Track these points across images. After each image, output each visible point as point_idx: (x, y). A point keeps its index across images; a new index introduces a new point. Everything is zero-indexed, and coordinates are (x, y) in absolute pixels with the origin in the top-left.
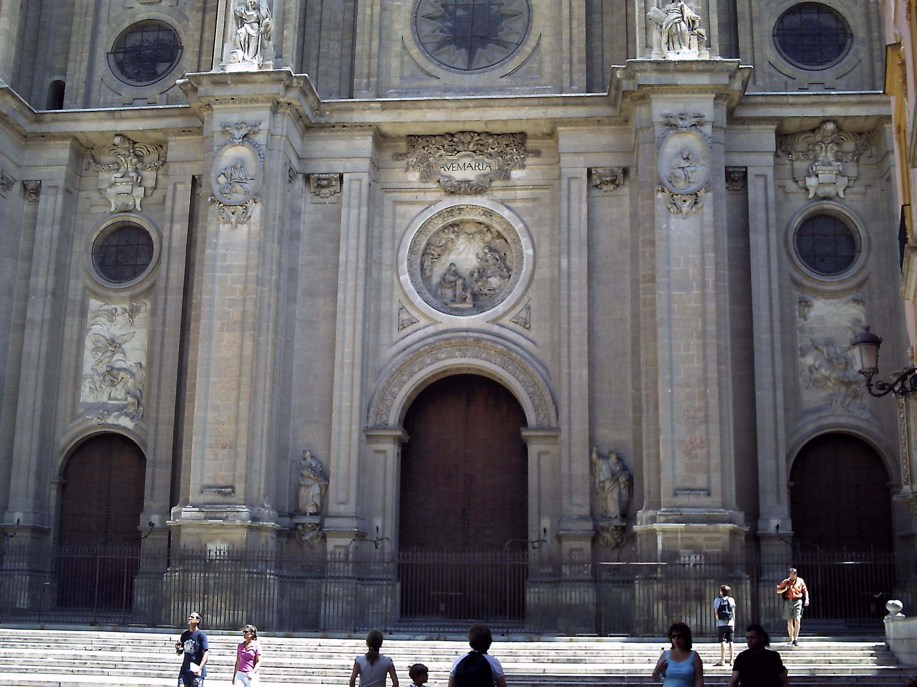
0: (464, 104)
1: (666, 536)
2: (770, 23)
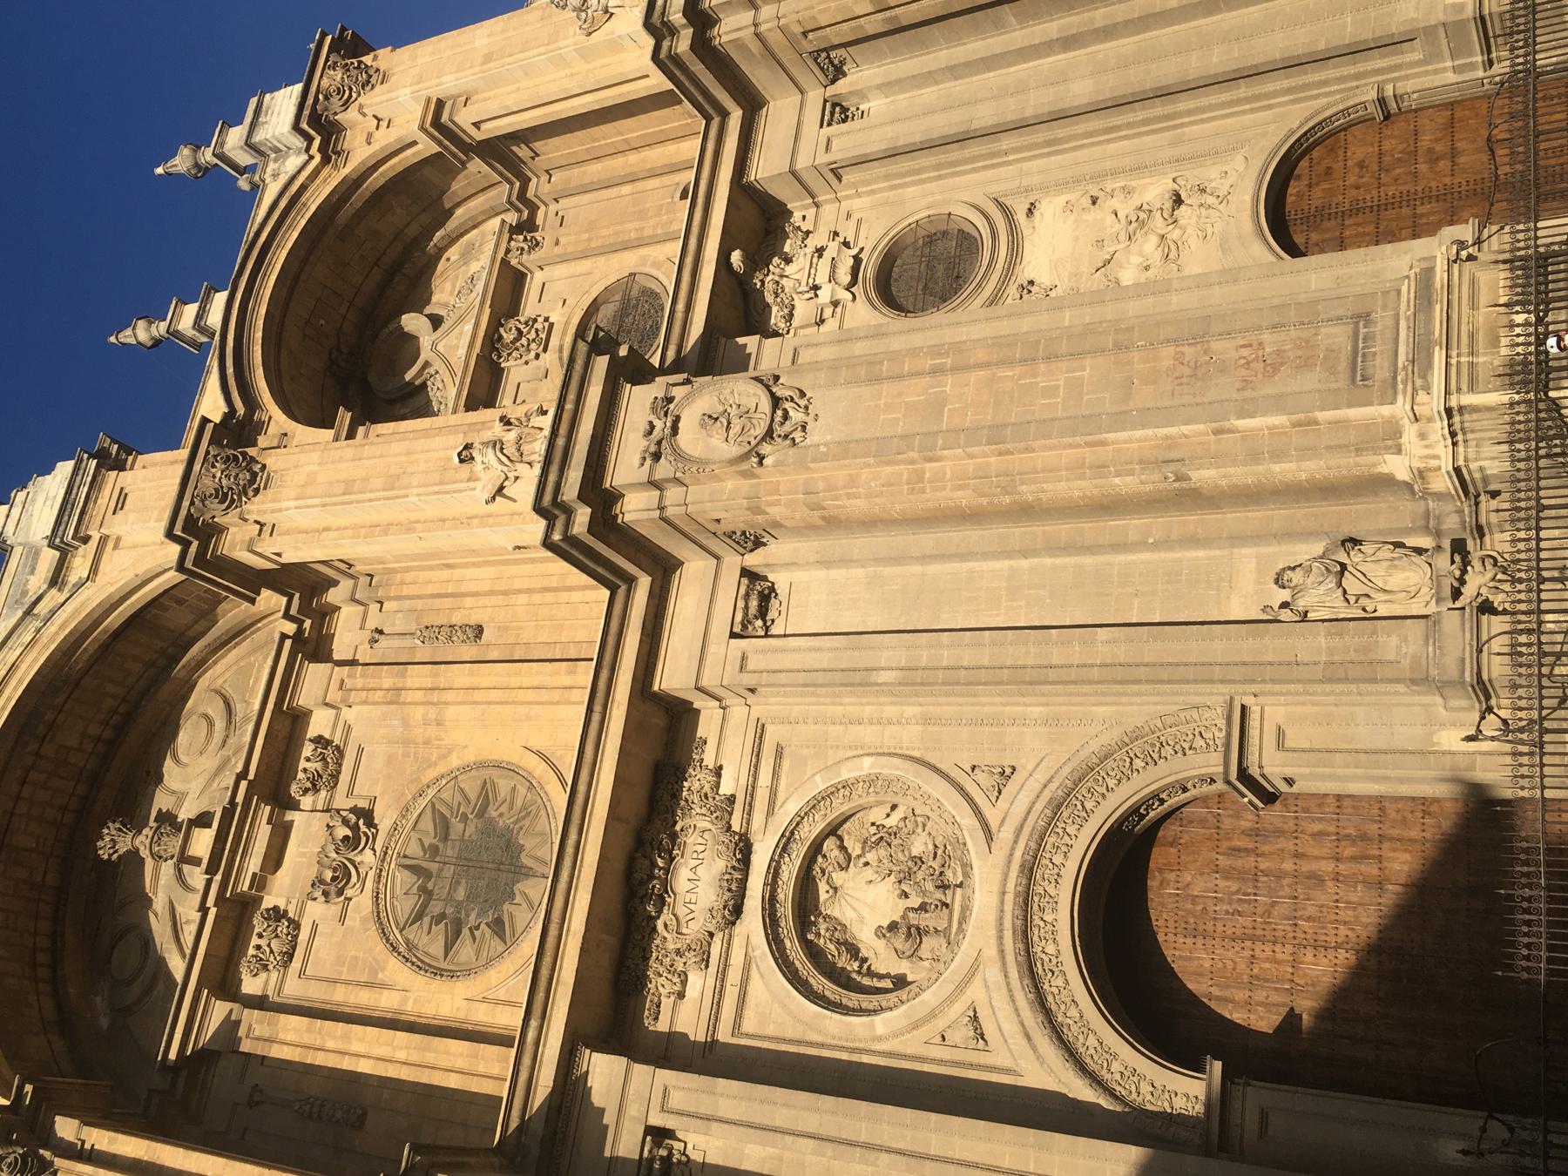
0: (570, 850)
1: (1464, 387)
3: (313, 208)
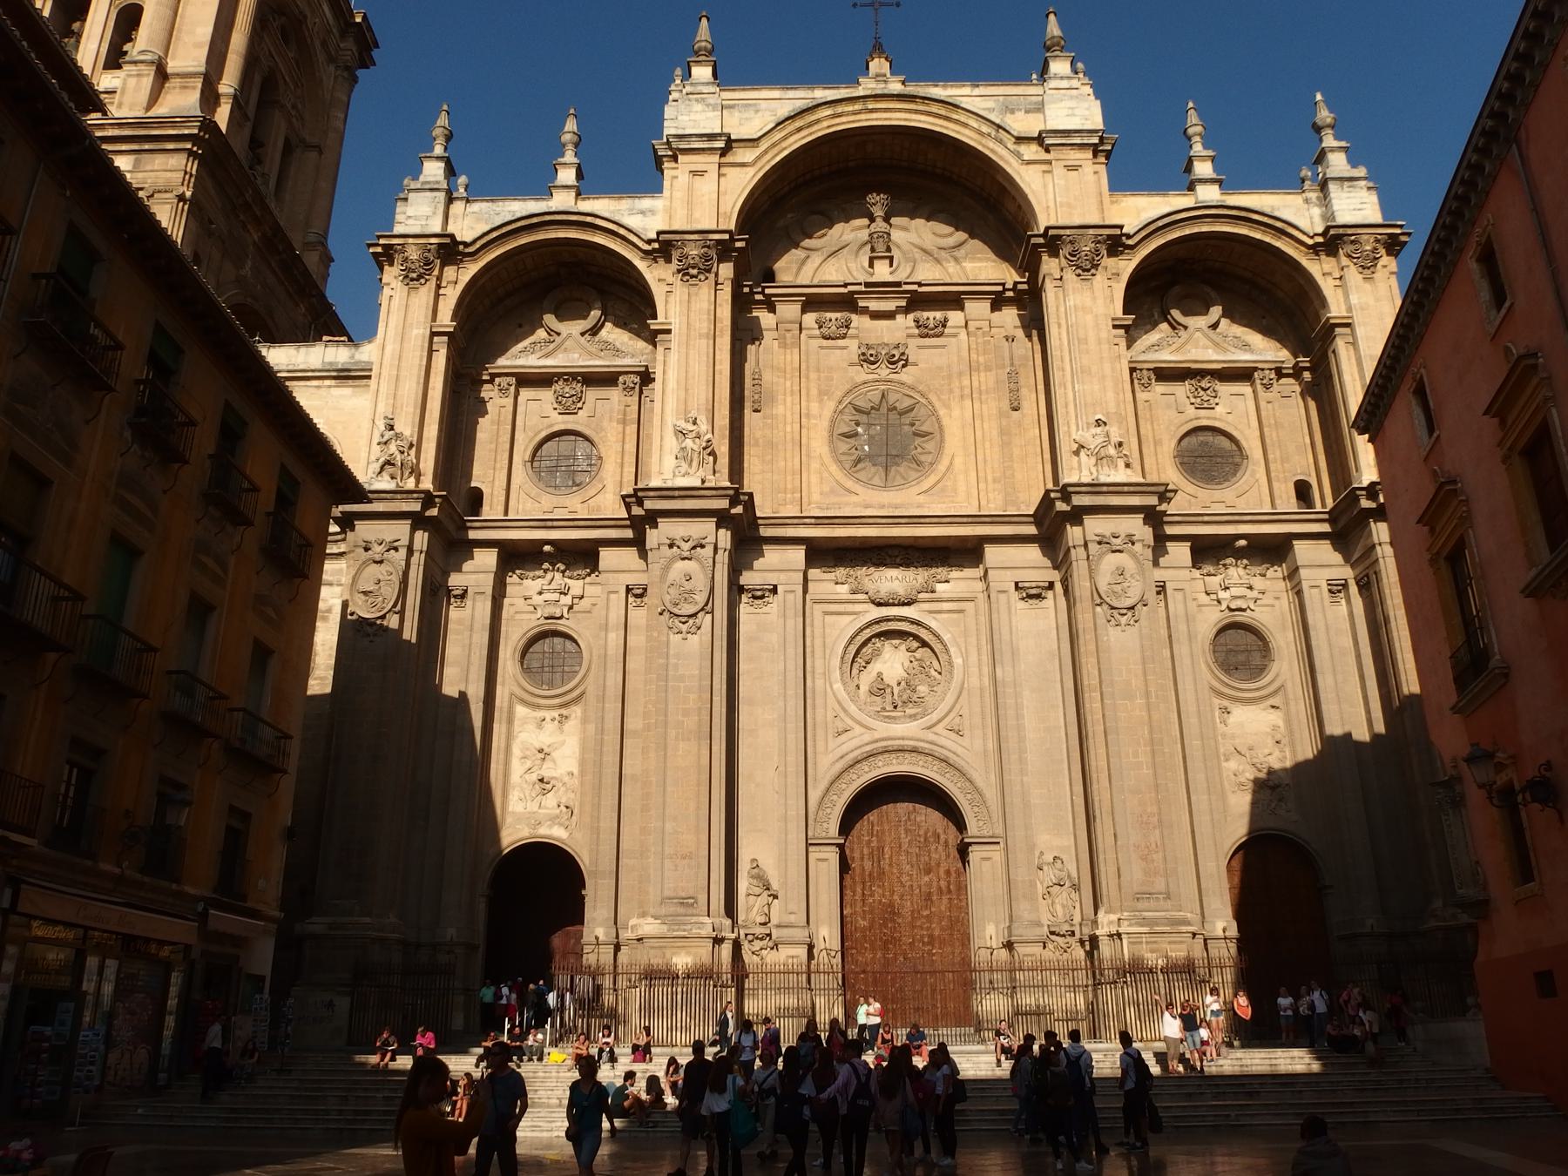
2: (1169, 446)
3: (1278, 244)
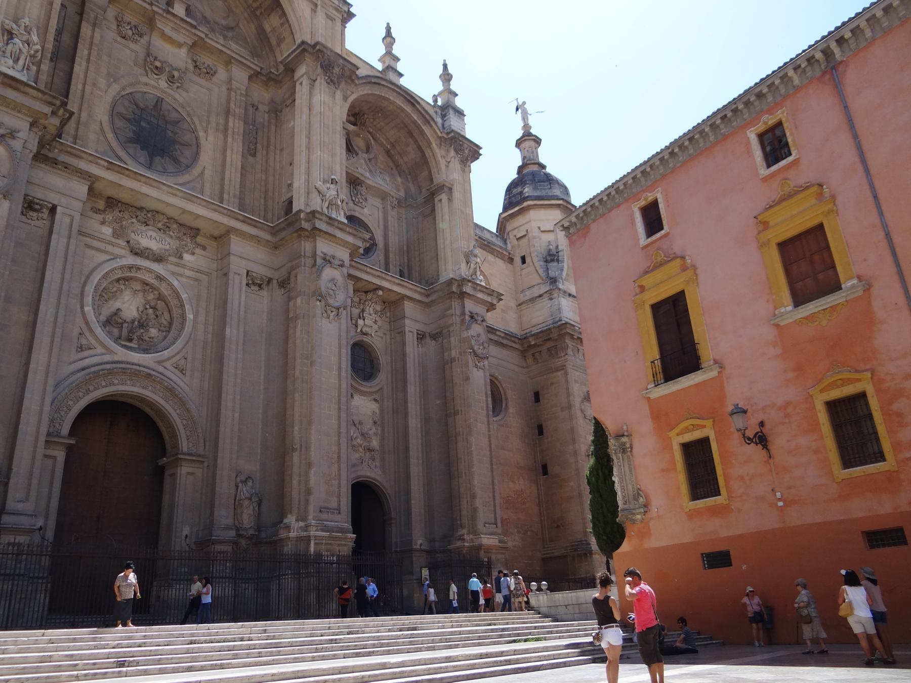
0: (175, 192)
